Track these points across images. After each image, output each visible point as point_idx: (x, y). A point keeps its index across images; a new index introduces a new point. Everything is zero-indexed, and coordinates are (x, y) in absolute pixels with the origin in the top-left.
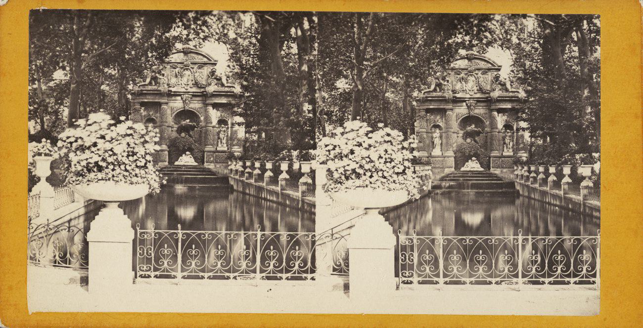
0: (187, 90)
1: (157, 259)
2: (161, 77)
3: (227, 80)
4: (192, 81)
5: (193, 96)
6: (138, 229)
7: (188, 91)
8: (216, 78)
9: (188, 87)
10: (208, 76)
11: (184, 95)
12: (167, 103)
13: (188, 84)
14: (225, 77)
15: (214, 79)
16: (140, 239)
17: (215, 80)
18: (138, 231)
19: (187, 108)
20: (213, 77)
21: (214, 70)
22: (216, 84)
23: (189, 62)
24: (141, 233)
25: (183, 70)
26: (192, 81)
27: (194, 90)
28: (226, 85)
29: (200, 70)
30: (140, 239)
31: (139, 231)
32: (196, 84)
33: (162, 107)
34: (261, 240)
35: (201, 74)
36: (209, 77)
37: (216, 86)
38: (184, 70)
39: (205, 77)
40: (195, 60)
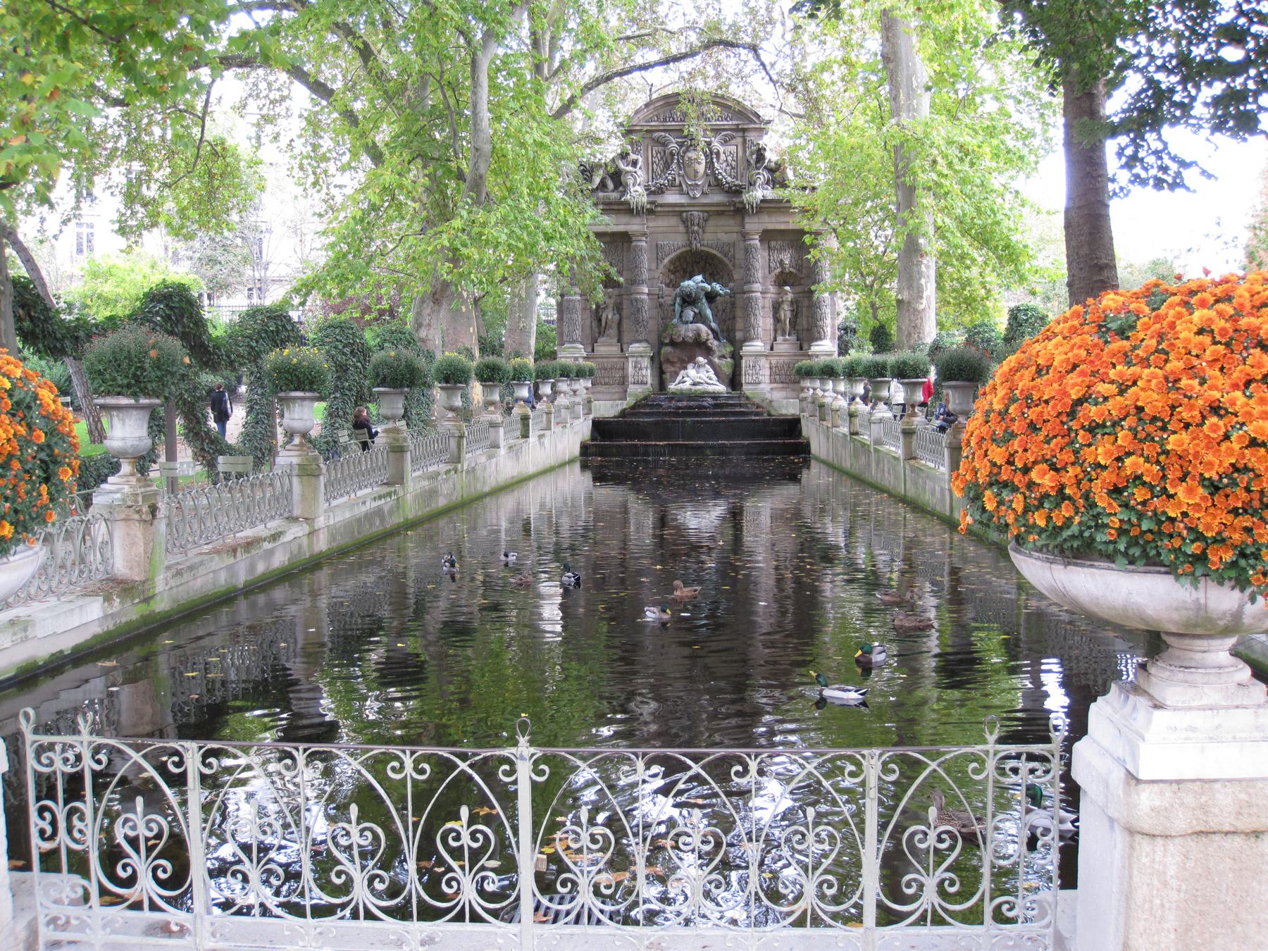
1: (112, 856)
6: (26, 728)
16: (38, 775)
18: (29, 737)
19: (696, 245)
24: (40, 750)
27: (717, 198)
30: (38, 775)
31: (31, 739)
34: (534, 784)
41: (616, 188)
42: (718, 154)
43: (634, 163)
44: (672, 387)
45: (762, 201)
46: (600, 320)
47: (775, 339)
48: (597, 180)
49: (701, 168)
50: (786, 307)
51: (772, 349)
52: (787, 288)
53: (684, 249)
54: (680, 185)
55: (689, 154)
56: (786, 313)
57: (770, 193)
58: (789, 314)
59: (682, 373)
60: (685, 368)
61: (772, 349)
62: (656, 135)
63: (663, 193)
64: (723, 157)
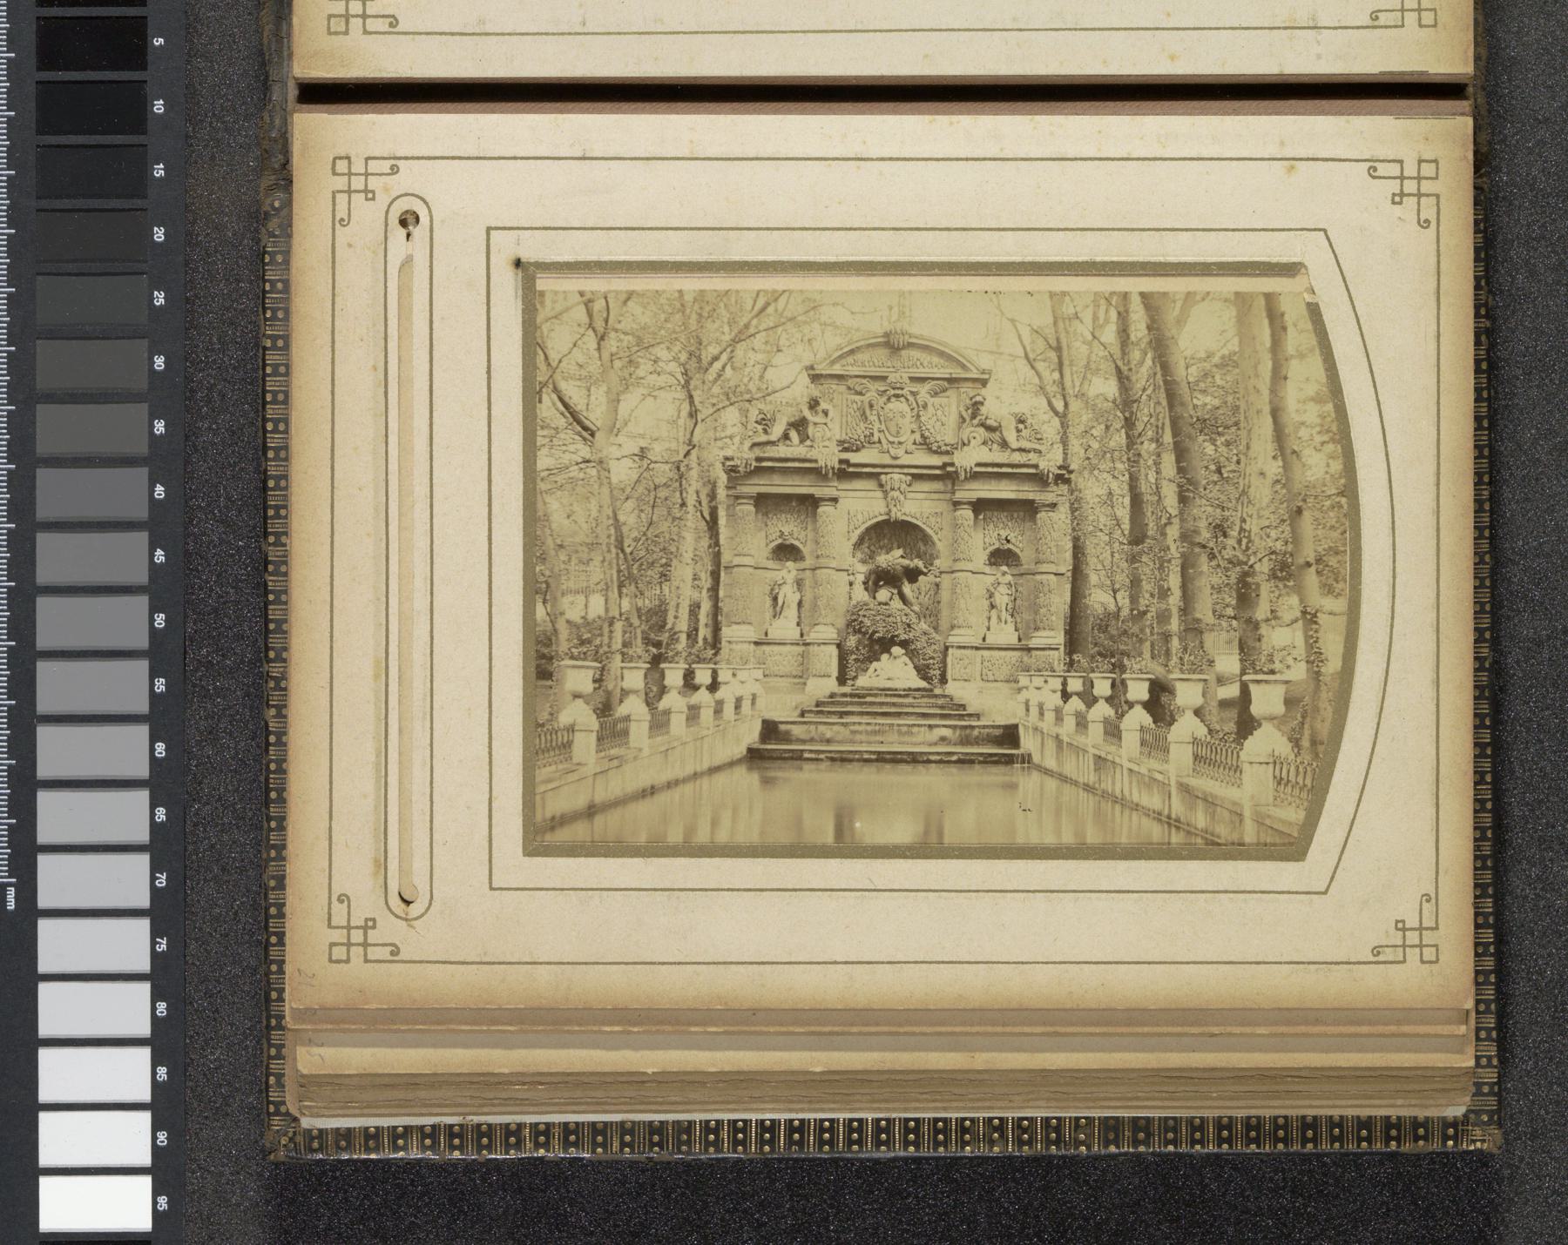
0: (896, 458)
2: (819, 419)
3: (1018, 431)
4: (913, 432)
5: (916, 477)
7: (898, 462)
8: (983, 425)
9: (900, 452)
10: (962, 417)
11: (886, 474)
12: (835, 500)
13: (900, 443)
14: (1014, 424)
15: (978, 426)
17: (982, 430)
19: (898, 514)
20: (975, 422)
21: (978, 399)
22: (984, 443)
23: (905, 376)
25: (884, 399)
26: (913, 432)
28: (1013, 442)
29: (937, 400)
32: (926, 444)
33: (820, 510)
35: (939, 413)
36: (964, 420)
37: (985, 449)
38: (889, 399)
39: (953, 419)
40: (922, 370)
41: (802, 442)
42: (925, 406)
43: (826, 413)
44: (863, 681)
45: (978, 465)
46: (775, 599)
47: (989, 629)
48: (777, 431)
49: (907, 423)
50: (1003, 589)
51: (984, 639)
52: (1004, 568)
53: (880, 518)
54: (880, 442)
55: (890, 406)
56: (1002, 599)
57: (985, 455)
58: (1006, 599)
59: (875, 664)
60: (878, 660)
61: (984, 639)
62: (851, 382)
63: (858, 450)
64: (930, 408)
